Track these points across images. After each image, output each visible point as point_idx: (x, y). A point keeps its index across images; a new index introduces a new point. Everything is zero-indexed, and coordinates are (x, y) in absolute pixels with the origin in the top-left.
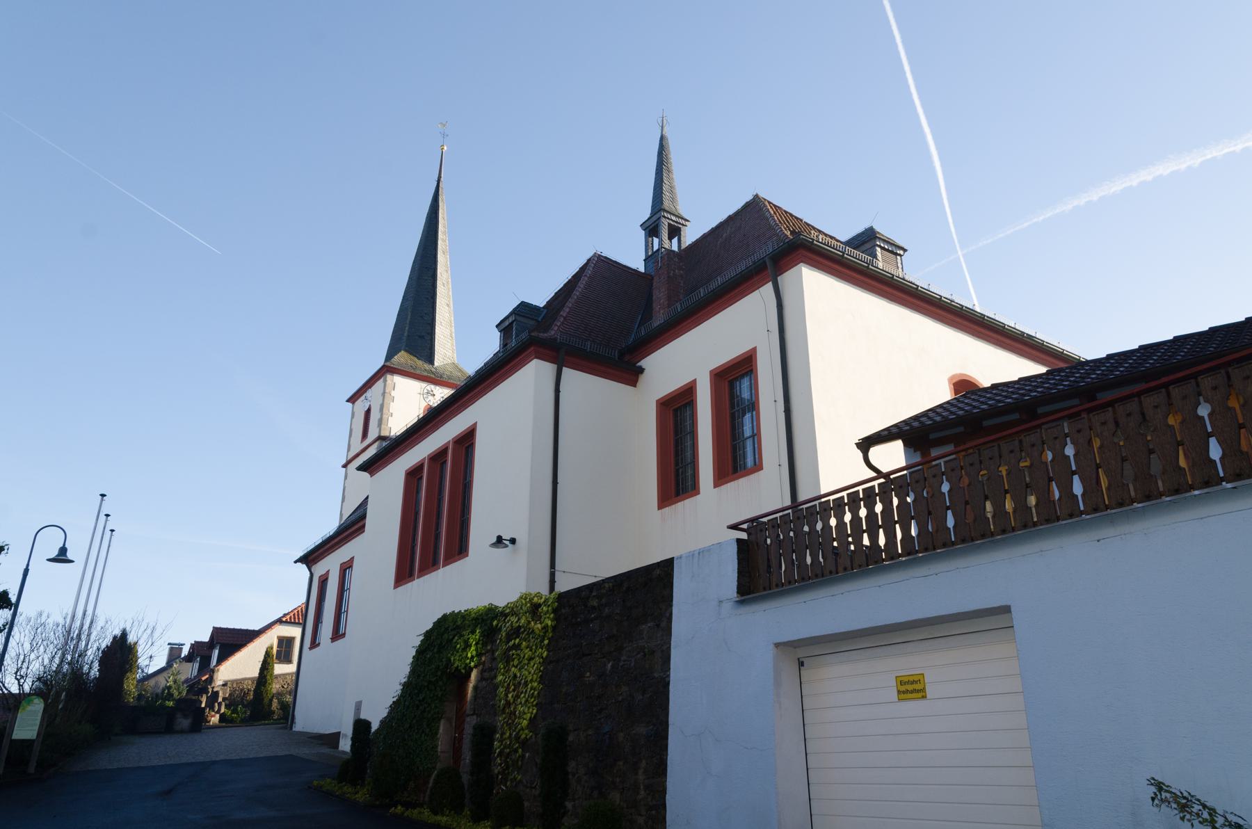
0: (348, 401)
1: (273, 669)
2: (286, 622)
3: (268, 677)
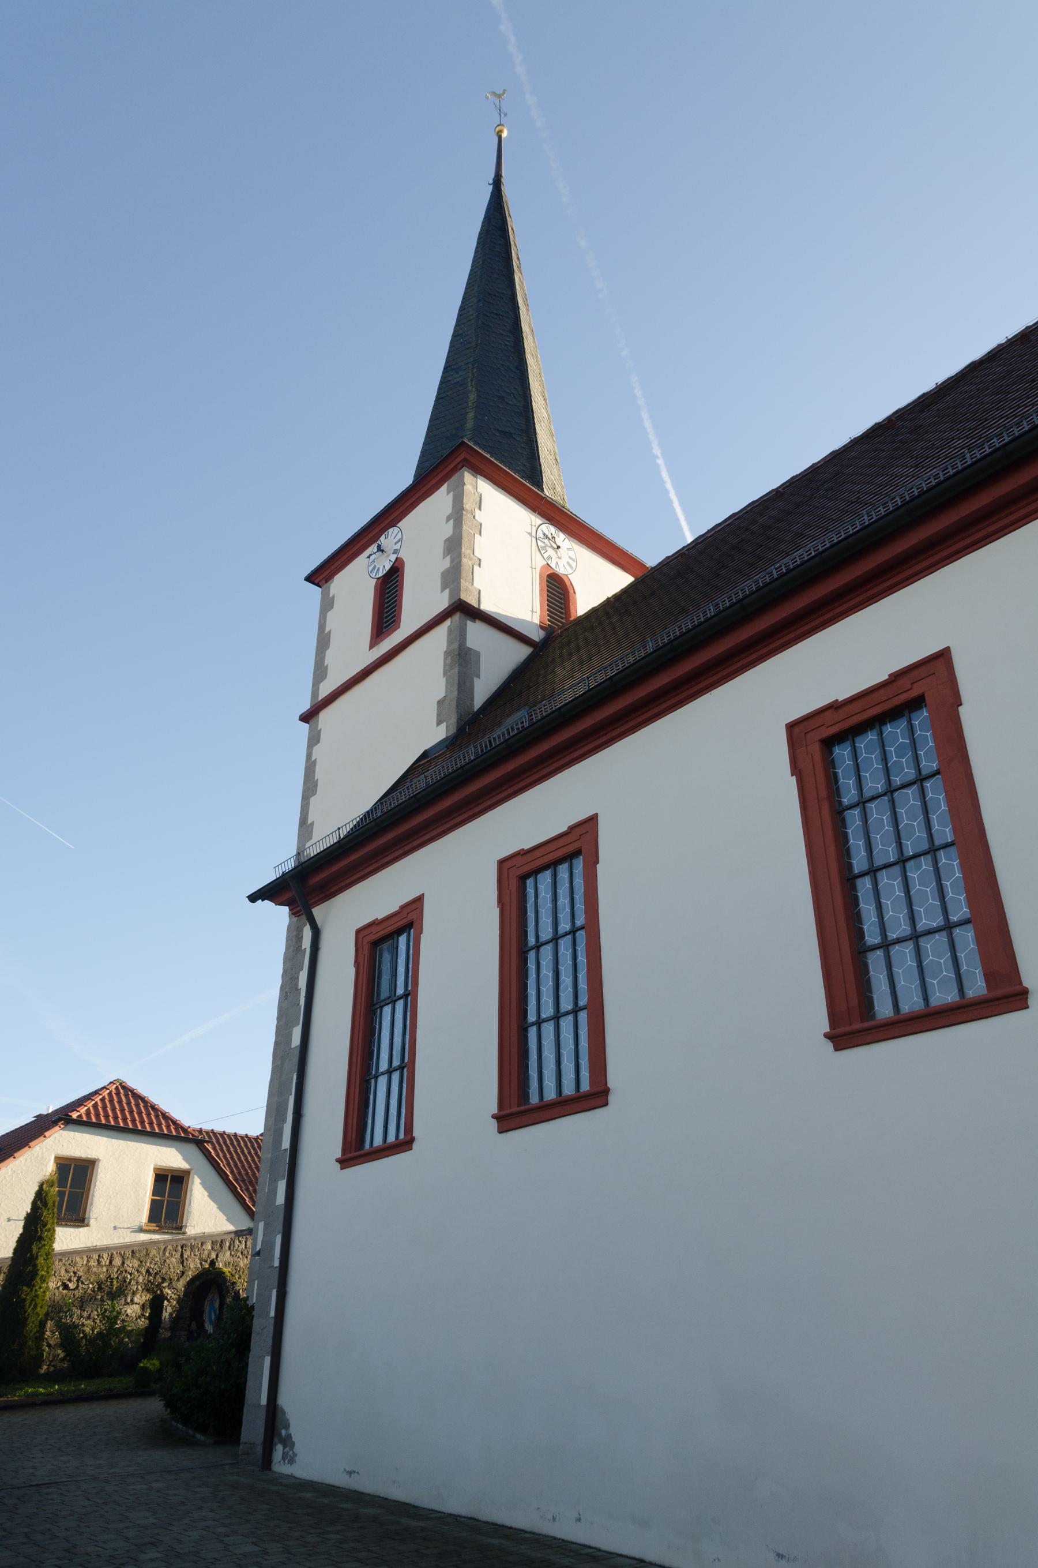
0: (311, 578)
1: (52, 1239)
2: (79, 1123)
3: (41, 1261)
